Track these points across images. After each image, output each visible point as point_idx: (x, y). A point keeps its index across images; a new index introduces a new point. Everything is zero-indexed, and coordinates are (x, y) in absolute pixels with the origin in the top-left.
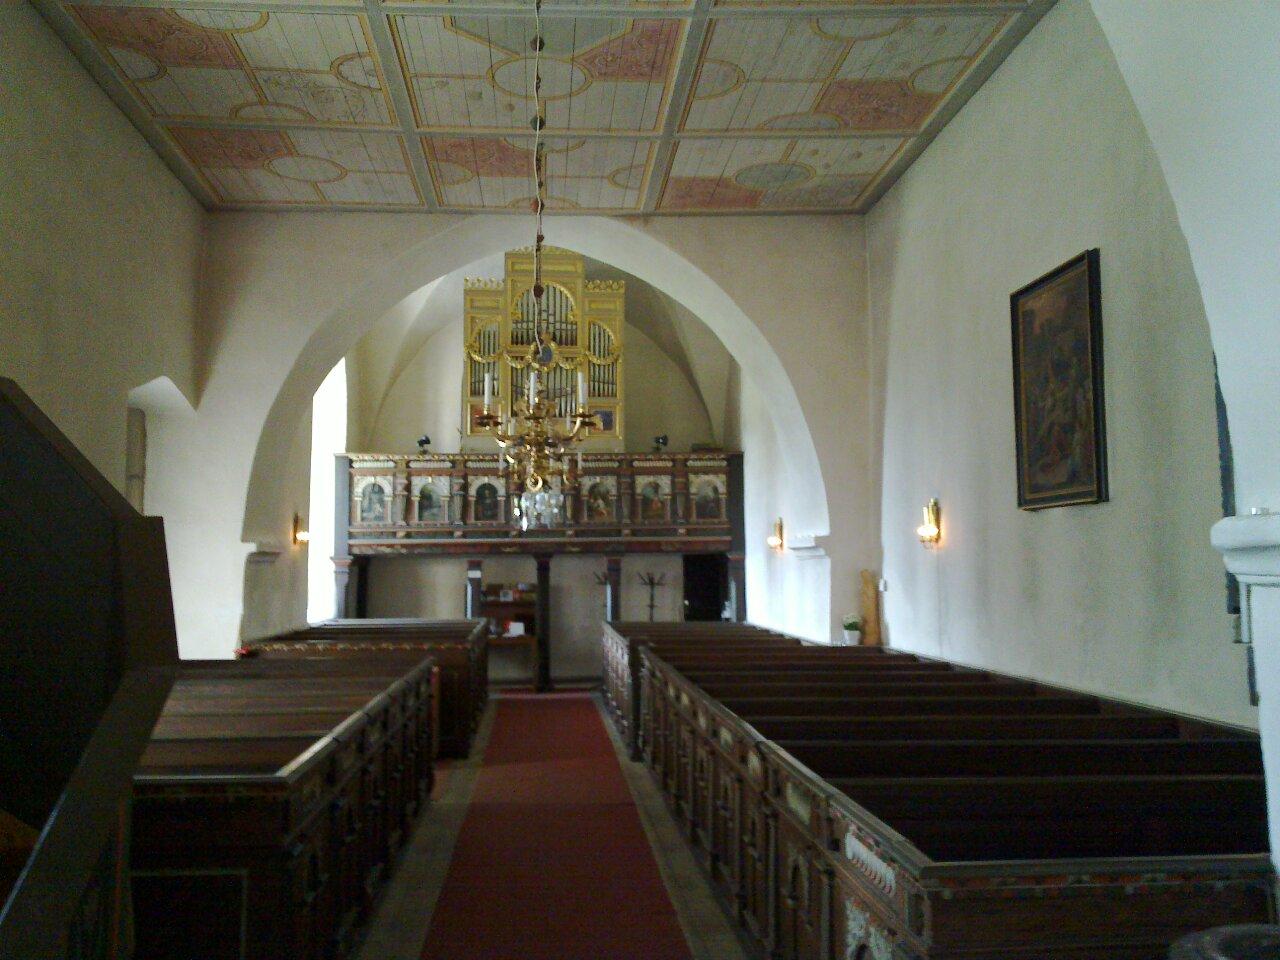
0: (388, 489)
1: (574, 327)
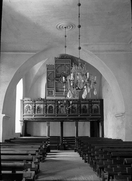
0: (31, 107)
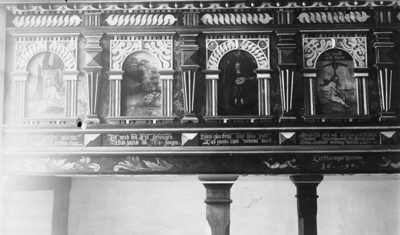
0: (70, 63)
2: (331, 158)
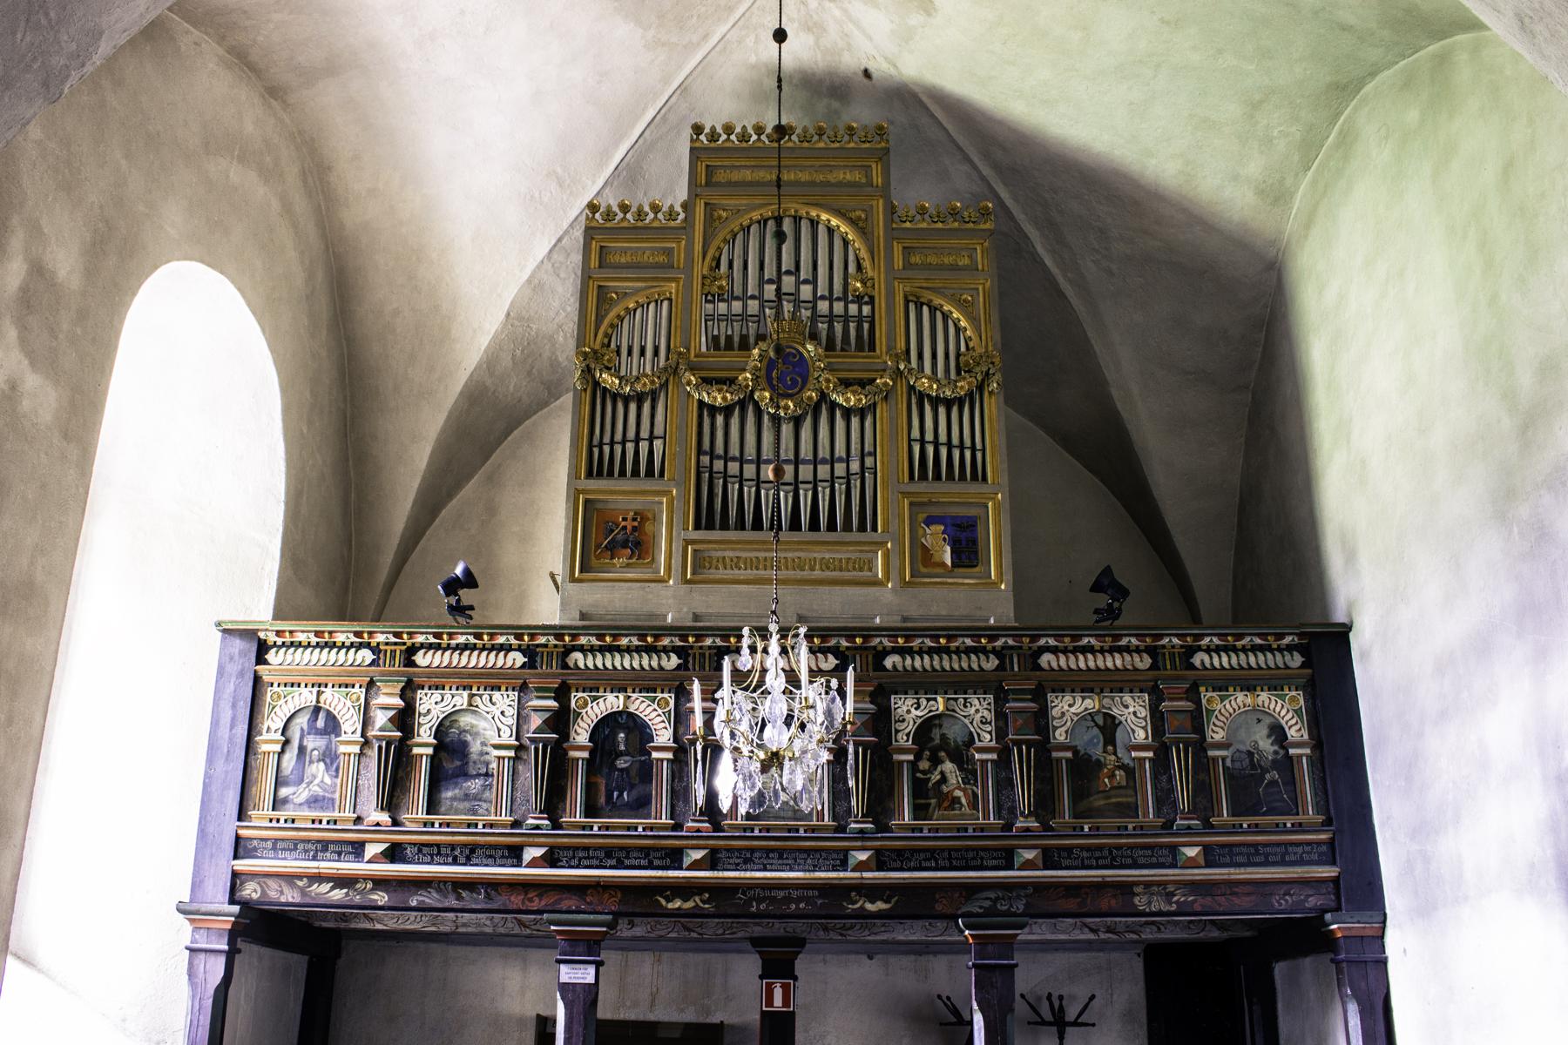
0: (350, 724)
1: (866, 310)
2: (767, 893)
